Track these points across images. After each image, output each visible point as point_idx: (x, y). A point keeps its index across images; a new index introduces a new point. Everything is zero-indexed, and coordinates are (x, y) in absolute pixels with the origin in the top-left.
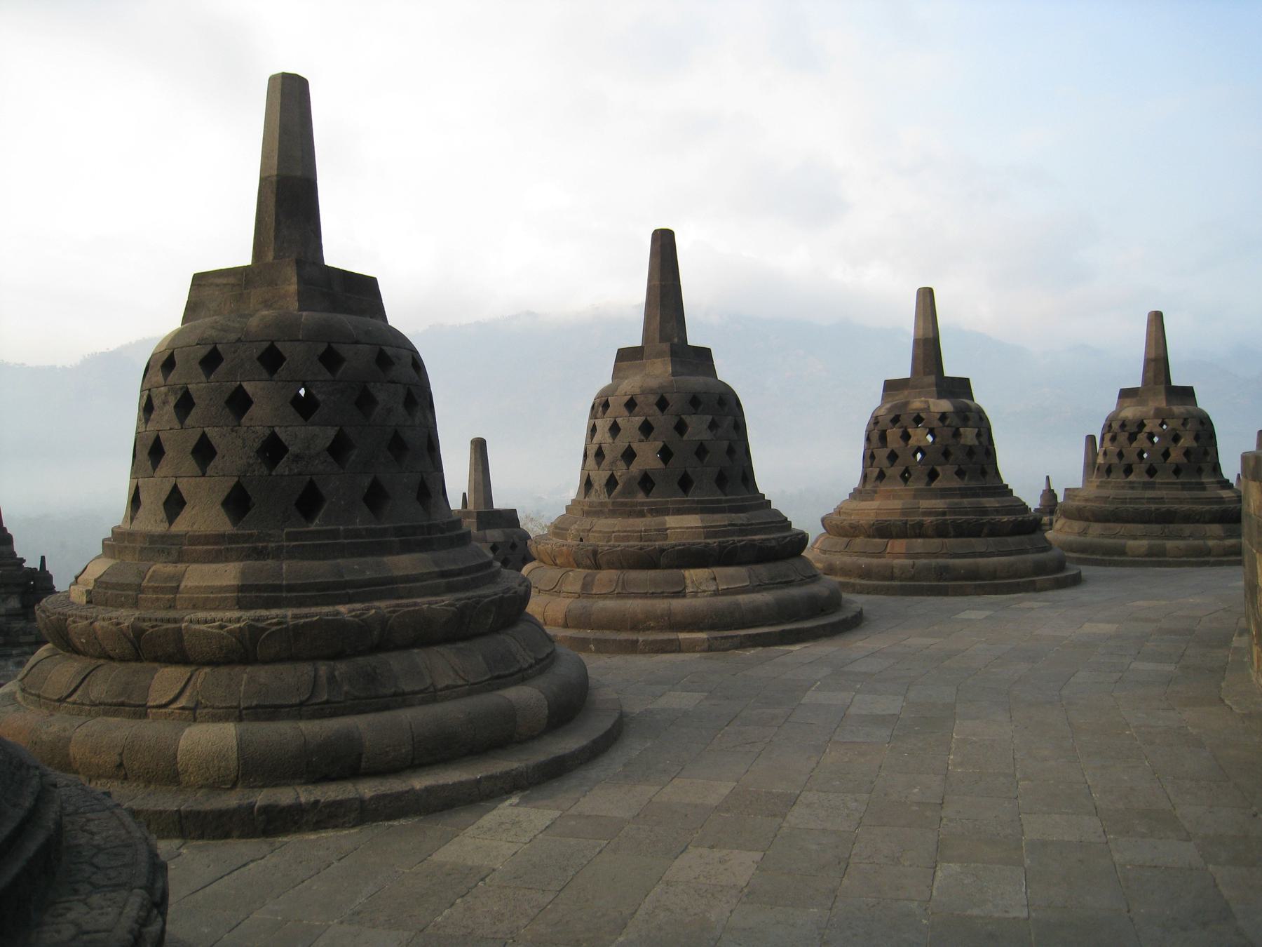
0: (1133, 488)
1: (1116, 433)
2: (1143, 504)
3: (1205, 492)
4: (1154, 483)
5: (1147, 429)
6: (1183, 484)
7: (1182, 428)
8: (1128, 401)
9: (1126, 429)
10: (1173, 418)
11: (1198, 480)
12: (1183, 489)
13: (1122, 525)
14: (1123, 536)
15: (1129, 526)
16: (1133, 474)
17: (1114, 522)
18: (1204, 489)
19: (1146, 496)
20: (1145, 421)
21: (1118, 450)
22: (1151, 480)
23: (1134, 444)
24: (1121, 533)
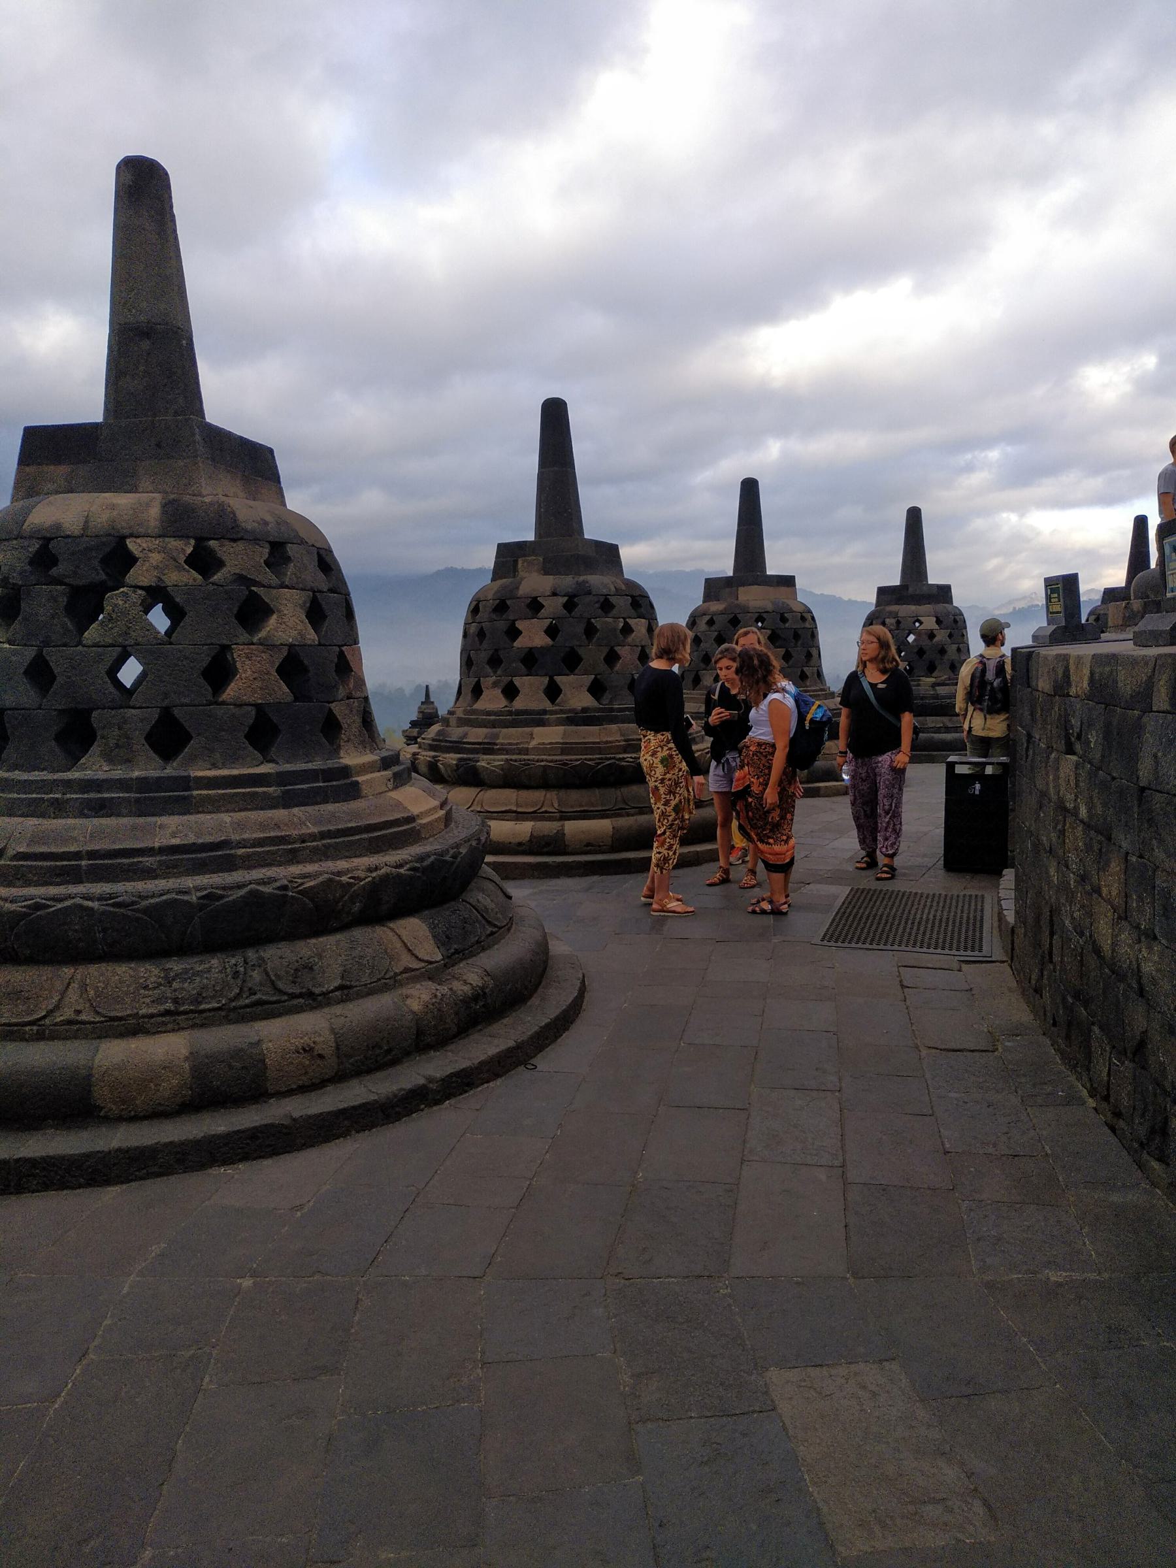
0: (101, 808)
1: (17, 589)
2: (149, 874)
3: (354, 805)
4: (186, 783)
5: (140, 575)
6: (282, 779)
7: (268, 576)
8: (60, 471)
9: (54, 571)
10: (234, 540)
11: (331, 764)
12: (288, 801)
13: (67, 971)
14: (74, 1030)
15: (95, 973)
16: (95, 749)
17: (31, 961)
18: (353, 792)
19: (157, 845)
20: (131, 544)
21: (30, 653)
22: (169, 771)
23: (92, 633)
24: (67, 1014)
